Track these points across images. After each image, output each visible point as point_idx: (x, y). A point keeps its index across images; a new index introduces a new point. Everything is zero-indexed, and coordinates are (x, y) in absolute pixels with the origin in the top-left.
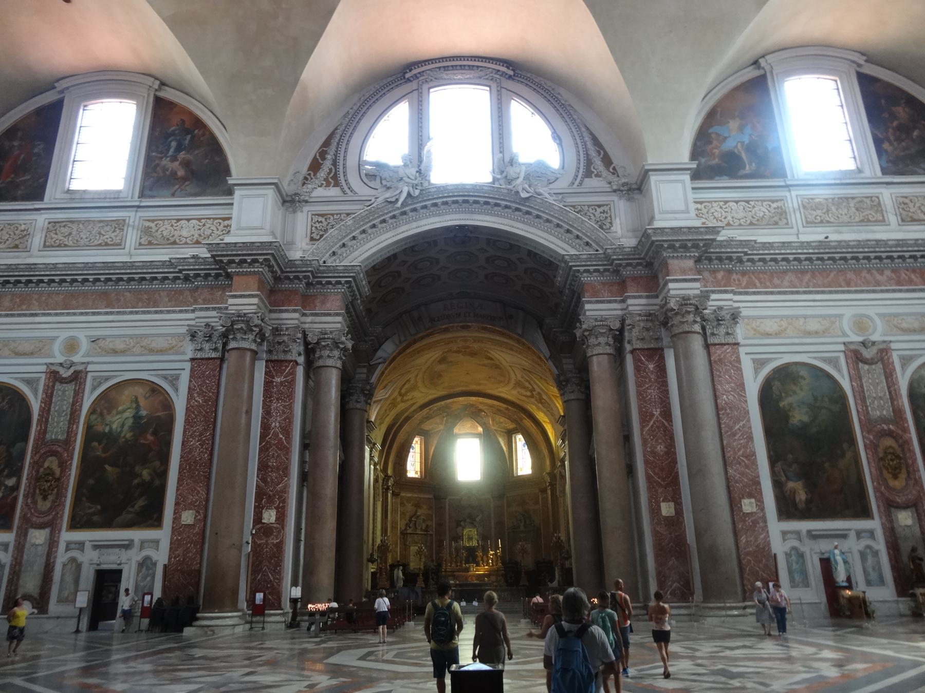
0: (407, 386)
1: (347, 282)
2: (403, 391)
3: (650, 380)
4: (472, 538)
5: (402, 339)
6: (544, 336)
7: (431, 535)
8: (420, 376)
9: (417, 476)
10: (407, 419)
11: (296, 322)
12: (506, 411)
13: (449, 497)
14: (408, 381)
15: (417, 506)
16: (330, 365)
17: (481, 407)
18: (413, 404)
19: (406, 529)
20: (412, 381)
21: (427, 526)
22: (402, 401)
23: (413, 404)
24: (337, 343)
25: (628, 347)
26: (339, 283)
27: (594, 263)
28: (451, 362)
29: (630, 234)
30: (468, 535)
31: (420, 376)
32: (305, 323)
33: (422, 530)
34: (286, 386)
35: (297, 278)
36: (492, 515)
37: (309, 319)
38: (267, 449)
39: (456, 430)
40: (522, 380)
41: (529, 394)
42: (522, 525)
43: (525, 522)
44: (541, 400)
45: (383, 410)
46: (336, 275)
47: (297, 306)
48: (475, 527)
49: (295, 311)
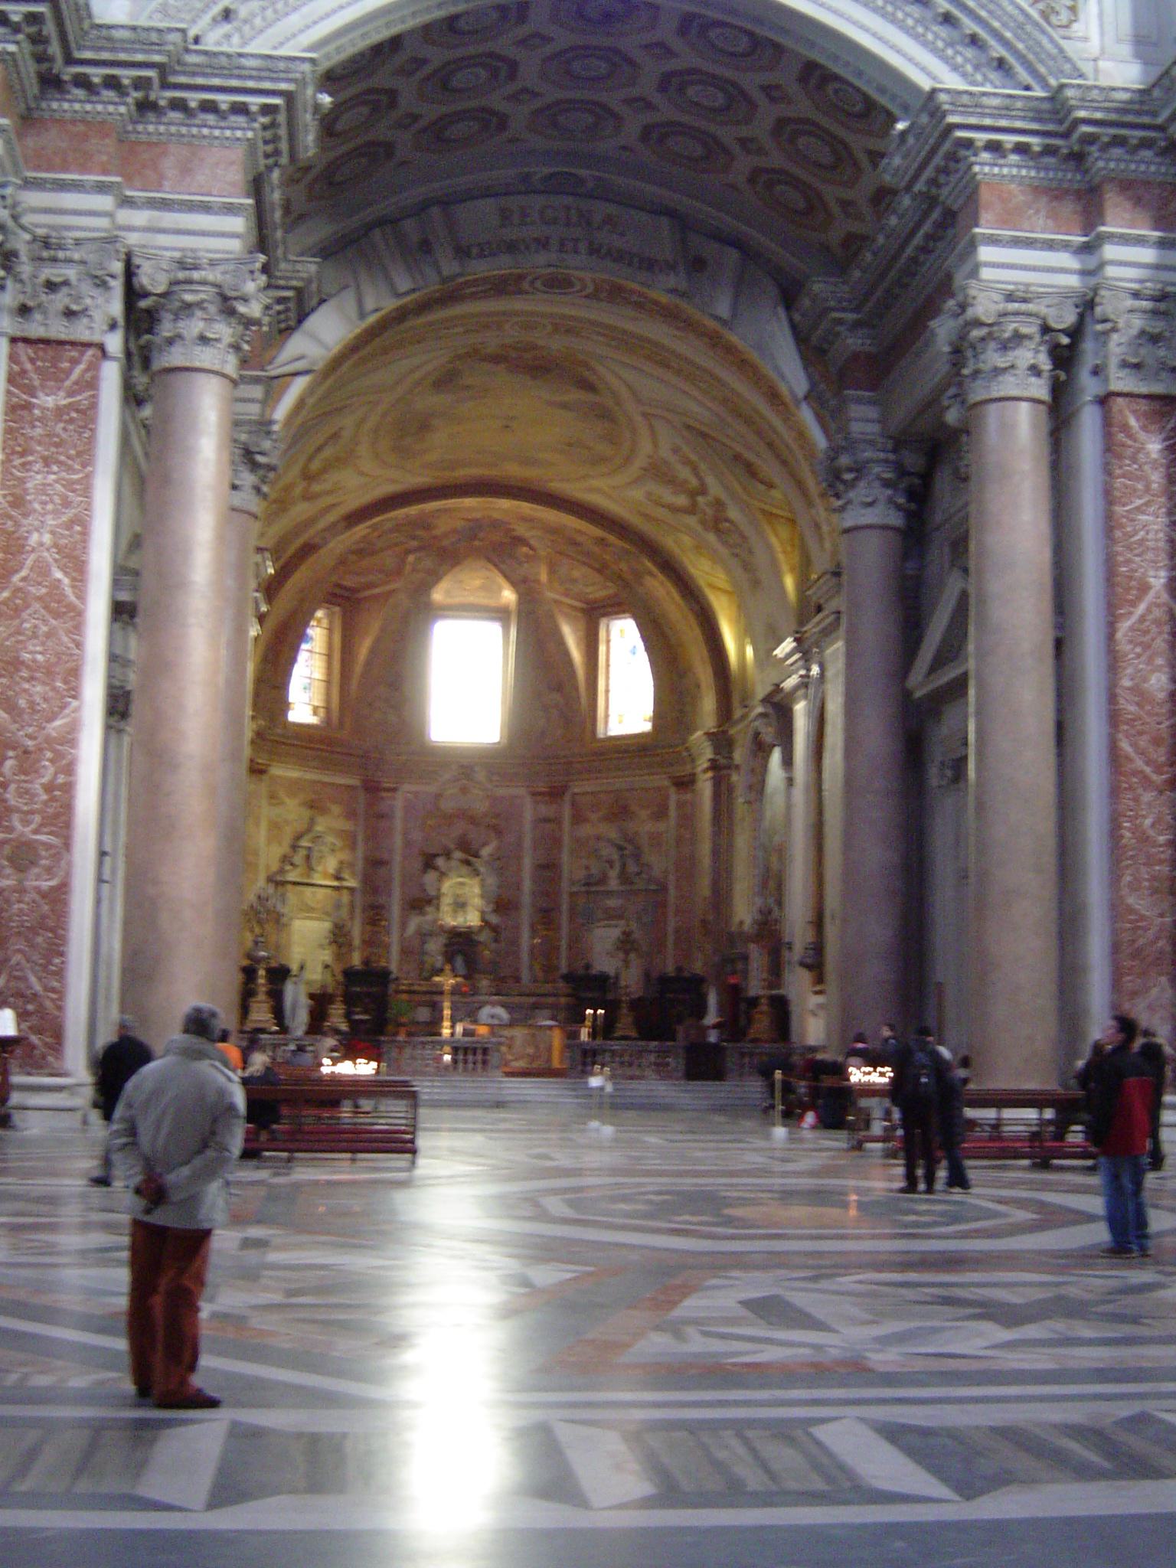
0: (328, 452)
1: (267, 110)
2: (315, 465)
3: (1147, 489)
5: (370, 303)
6: (794, 327)
9: (313, 720)
11: (103, 222)
12: (596, 549)
13: (406, 787)
15: (315, 806)
16: (206, 365)
17: (521, 530)
19: (281, 871)
22: (307, 497)
24: (225, 299)
25: (1089, 387)
26: (240, 109)
27: (1019, 124)
28: (468, 387)
29: (1126, 50)
32: (130, 229)
33: (325, 875)
34: (71, 421)
35: (112, 83)
36: (527, 843)
37: (140, 217)
38: (17, 611)
39: (438, 595)
40: (672, 459)
41: (682, 500)
42: (613, 874)
43: (624, 866)
44: (718, 523)
46: (234, 83)
47: (105, 172)
48: (476, 873)
49: (101, 188)
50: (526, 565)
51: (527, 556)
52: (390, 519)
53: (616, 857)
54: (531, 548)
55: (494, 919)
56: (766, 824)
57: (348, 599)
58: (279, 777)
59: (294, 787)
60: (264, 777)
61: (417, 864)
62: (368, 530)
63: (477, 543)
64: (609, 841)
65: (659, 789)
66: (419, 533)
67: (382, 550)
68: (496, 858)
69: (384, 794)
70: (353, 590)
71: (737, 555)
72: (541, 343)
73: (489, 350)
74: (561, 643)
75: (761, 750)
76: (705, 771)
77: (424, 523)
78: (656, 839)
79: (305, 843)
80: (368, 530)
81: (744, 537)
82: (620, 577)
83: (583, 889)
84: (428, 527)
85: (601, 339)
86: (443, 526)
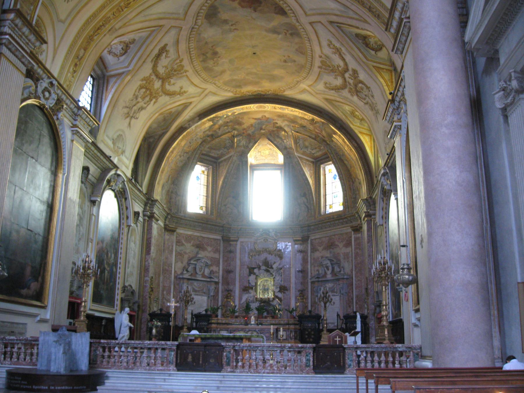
0: (164, 62)
4: (268, 289)
7: (217, 283)
8: (183, 46)
9: (201, 212)
10: (181, 130)
12: (311, 127)
13: (241, 240)
14: (163, 50)
15: (200, 247)
17: (280, 123)
18: (186, 106)
19: (182, 274)
21: (212, 272)
23: (186, 106)
28: (226, 22)
30: (264, 285)
31: (183, 46)
33: (203, 276)
41: (339, 82)
42: (329, 272)
43: (333, 269)
45: (129, 93)
51: (284, 136)
52: (220, 117)
53: (329, 264)
54: (285, 131)
55: (280, 295)
57: (215, 162)
58: (181, 234)
59: (189, 238)
60: (175, 233)
62: (211, 123)
63: (263, 131)
64: (327, 257)
65: (346, 233)
66: (237, 127)
69: (232, 243)
70: (217, 159)
71: (367, 103)
76: (364, 219)
77: (237, 121)
78: (346, 256)
79: (192, 262)
80: (211, 123)
81: (368, 88)
83: (317, 280)
84: (240, 124)
86: (247, 122)
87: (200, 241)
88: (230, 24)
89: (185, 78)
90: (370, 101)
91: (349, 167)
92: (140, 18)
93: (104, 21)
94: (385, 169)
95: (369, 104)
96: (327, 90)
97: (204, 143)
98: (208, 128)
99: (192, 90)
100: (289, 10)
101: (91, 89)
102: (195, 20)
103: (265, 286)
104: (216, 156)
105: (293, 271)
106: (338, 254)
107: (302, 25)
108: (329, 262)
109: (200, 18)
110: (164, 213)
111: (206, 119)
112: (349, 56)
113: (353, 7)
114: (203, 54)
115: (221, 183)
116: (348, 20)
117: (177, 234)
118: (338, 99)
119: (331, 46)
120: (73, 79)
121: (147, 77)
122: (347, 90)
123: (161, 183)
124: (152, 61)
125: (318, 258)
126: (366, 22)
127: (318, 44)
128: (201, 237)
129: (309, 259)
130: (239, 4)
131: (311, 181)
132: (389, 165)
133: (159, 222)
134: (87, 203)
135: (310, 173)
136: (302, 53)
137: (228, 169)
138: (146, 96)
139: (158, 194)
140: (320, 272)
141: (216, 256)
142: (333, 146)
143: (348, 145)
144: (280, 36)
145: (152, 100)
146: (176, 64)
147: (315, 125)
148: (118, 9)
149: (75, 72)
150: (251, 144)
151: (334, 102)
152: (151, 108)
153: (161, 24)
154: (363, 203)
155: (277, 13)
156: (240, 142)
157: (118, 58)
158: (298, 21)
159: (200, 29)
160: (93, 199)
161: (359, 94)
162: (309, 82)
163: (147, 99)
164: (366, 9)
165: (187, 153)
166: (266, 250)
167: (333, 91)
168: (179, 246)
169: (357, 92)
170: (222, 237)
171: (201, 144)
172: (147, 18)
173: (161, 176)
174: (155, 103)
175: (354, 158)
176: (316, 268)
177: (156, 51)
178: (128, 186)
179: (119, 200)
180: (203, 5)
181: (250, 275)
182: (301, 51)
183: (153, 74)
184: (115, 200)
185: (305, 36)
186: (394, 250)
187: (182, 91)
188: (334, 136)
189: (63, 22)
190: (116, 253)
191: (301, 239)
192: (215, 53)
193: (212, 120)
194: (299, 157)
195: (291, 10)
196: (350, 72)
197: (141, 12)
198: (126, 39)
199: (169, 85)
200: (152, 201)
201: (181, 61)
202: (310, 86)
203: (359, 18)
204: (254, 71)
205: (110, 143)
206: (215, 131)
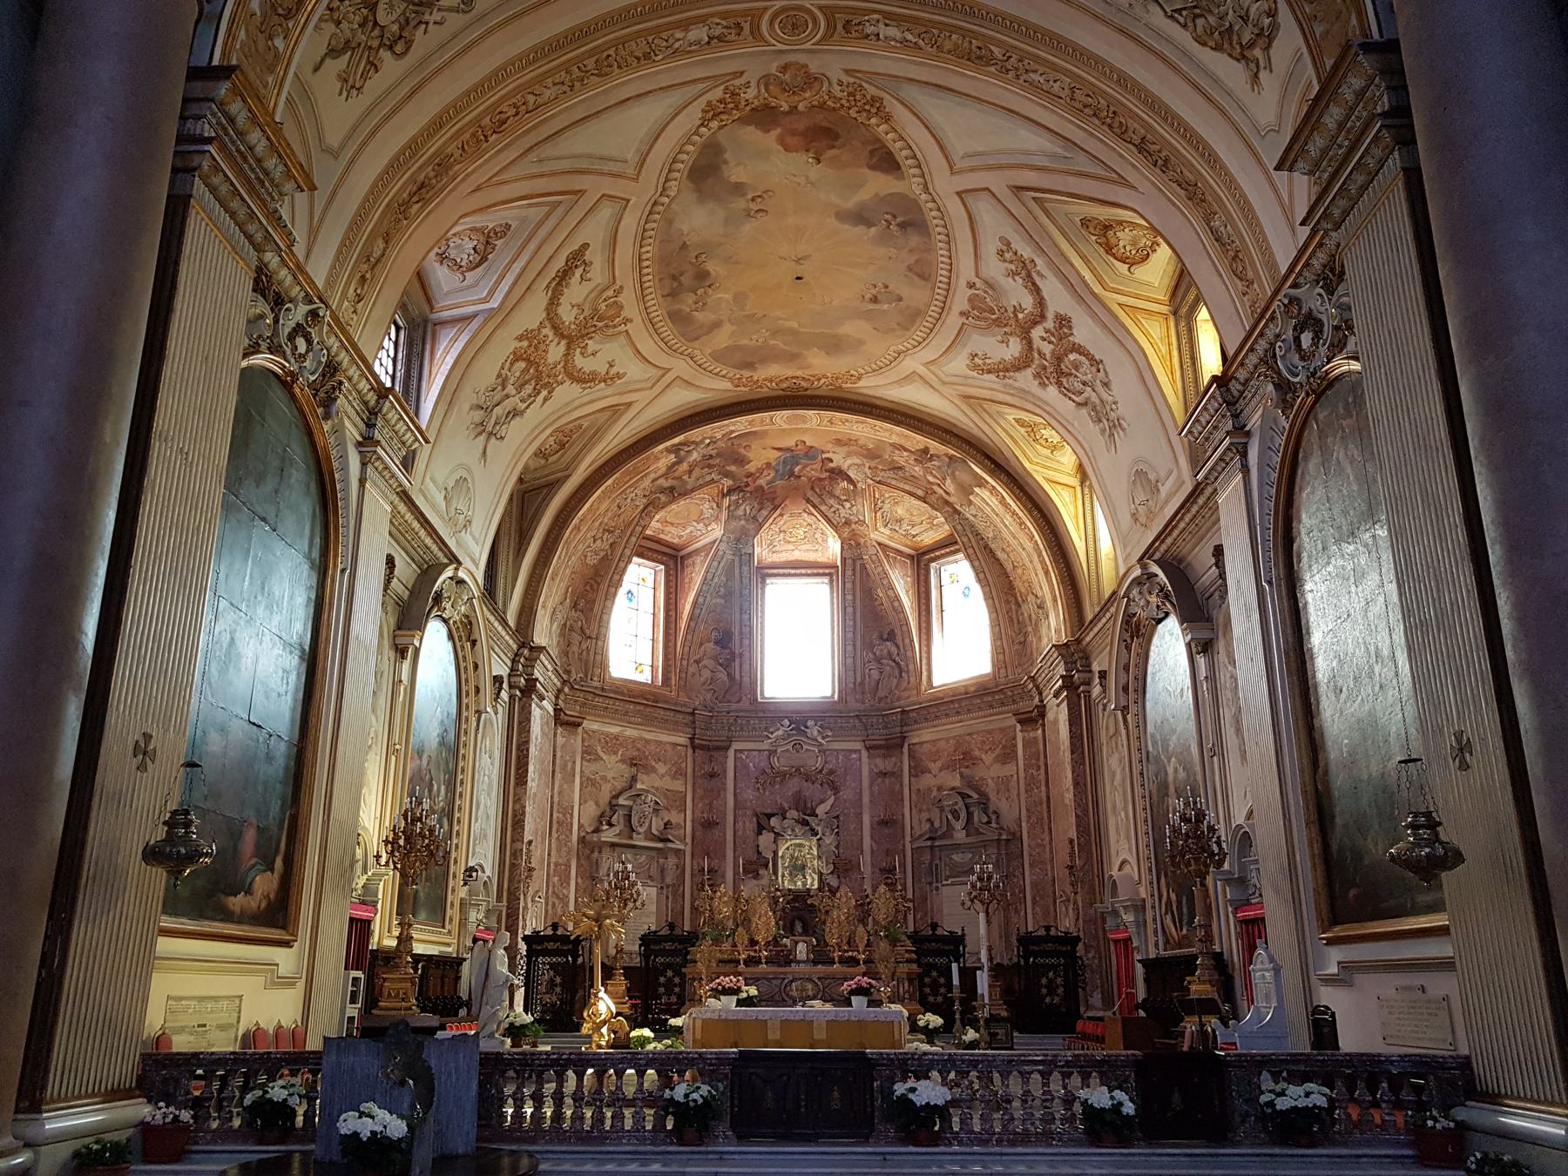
0: (576, 292)
12: (918, 470)
13: (736, 746)
14: (577, 259)
15: (637, 763)
17: (839, 459)
18: (616, 411)
20: (595, 256)
23: (616, 411)
28: (739, 189)
36: (866, 800)
39: (763, 550)
41: (1014, 348)
45: (486, 372)
50: (848, 505)
54: (850, 480)
56: (1150, 728)
59: (612, 743)
61: (751, 826)
62: (672, 458)
64: (953, 789)
65: (1002, 730)
66: (733, 468)
67: (692, 491)
68: (836, 821)
70: (676, 548)
71: (1085, 404)
72: (814, 68)
73: (751, 93)
74: (891, 587)
75: (1138, 633)
76: (1056, 695)
77: (732, 455)
79: (621, 801)
80: (672, 458)
81: (1096, 363)
82: (947, 503)
85: (893, 32)
87: (638, 750)
88: (750, 197)
89: (622, 339)
90: (1094, 398)
91: (1009, 567)
92: (528, 166)
93: (439, 165)
94: (1144, 567)
95: (1090, 406)
96: (975, 374)
97: (650, 508)
98: (660, 472)
99: (634, 370)
100: (907, 158)
101: (392, 353)
102: (662, 180)
103: (797, 859)
104: (676, 541)
105: (866, 820)
106: (982, 779)
107: (937, 199)
108: (961, 803)
109: (677, 175)
110: (556, 681)
111: (661, 447)
112: (1054, 279)
113: (1092, 146)
114: (674, 278)
115: (688, 607)
116: (1071, 179)
117: (585, 731)
118: (1001, 397)
119: (1008, 256)
120: (355, 318)
121: (532, 331)
122: (1029, 372)
123: (550, 605)
124: (548, 287)
125: (930, 790)
126: (1123, 182)
127: (972, 251)
128: (642, 739)
129: (906, 791)
130: (781, 141)
131: (907, 602)
132: (1157, 556)
133: (545, 703)
134: (389, 653)
135: (906, 582)
136: (922, 277)
137: (707, 572)
138: (526, 383)
139: (544, 633)
140: (937, 824)
141: (677, 785)
142: (968, 516)
143: (1014, 513)
144: (873, 230)
145: (538, 393)
146: (605, 300)
147: (929, 465)
148: (474, 135)
149: (359, 298)
150: (765, 513)
151: (987, 405)
152: (537, 413)
153: (578, 188)
154: (1055, 655)
155: (872, 168)
156: (737, 507)
157: (462, 273)
158: (926, 189)
159: (673, 206)
160: (399, 641)
161: (1064, 380)
162: (929, 354)
163: (529, 389)
164: (1130, 146)
165: (610, 532)
166: (798, 770)
167: (992, 377)
168: (589, 761)
169: (1057, 373)
170: (692, 739)
171: (643, 511)
172: (546, 168)
173: (550, 589)
174: (545, 400)
175: (1029, 545)
176: (925, 815)
177: (559, 263)
178: (482, 613)
179: (458, 644)
180: (689, 142)
181: (760, 833)
182: (921, 272)
183: (547, 323)
184: (450, 645)
185: (939, 229)
186: (1170, 771)
187: (613, 371)
188: (977, 490)
189: (335, 155)
190: (451, 785)
191: (882, 743)
192: (702, 276)
193: (675, 450)
194: (879, 544)
195: (915, 157)
196: (1050, 324)
197: (530, 149)
198: (489, 221)
199: (582, 354)
200: (531, 649)
201: (618, 292)
202: (927, 364)
203: (1100, 171)
204: (795, 325)
205: (439, 498)
206: (680, 478)
